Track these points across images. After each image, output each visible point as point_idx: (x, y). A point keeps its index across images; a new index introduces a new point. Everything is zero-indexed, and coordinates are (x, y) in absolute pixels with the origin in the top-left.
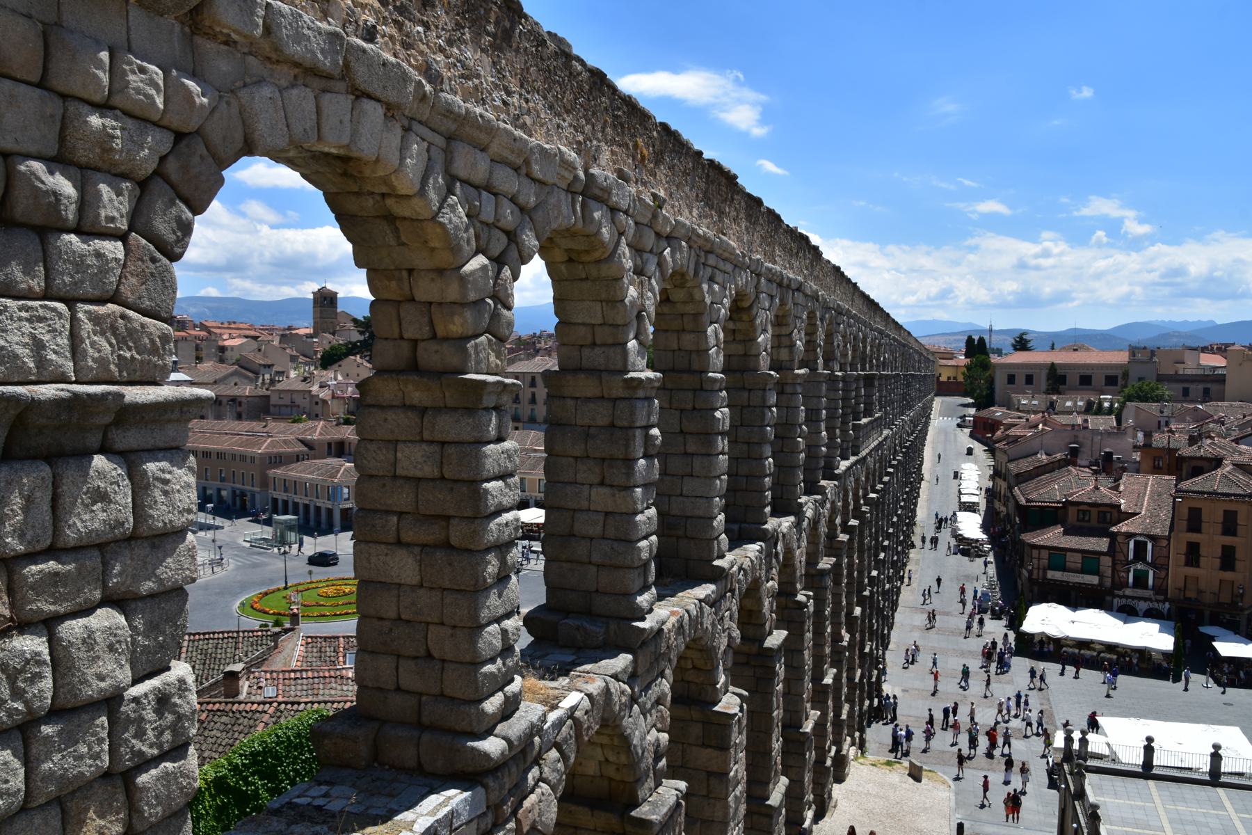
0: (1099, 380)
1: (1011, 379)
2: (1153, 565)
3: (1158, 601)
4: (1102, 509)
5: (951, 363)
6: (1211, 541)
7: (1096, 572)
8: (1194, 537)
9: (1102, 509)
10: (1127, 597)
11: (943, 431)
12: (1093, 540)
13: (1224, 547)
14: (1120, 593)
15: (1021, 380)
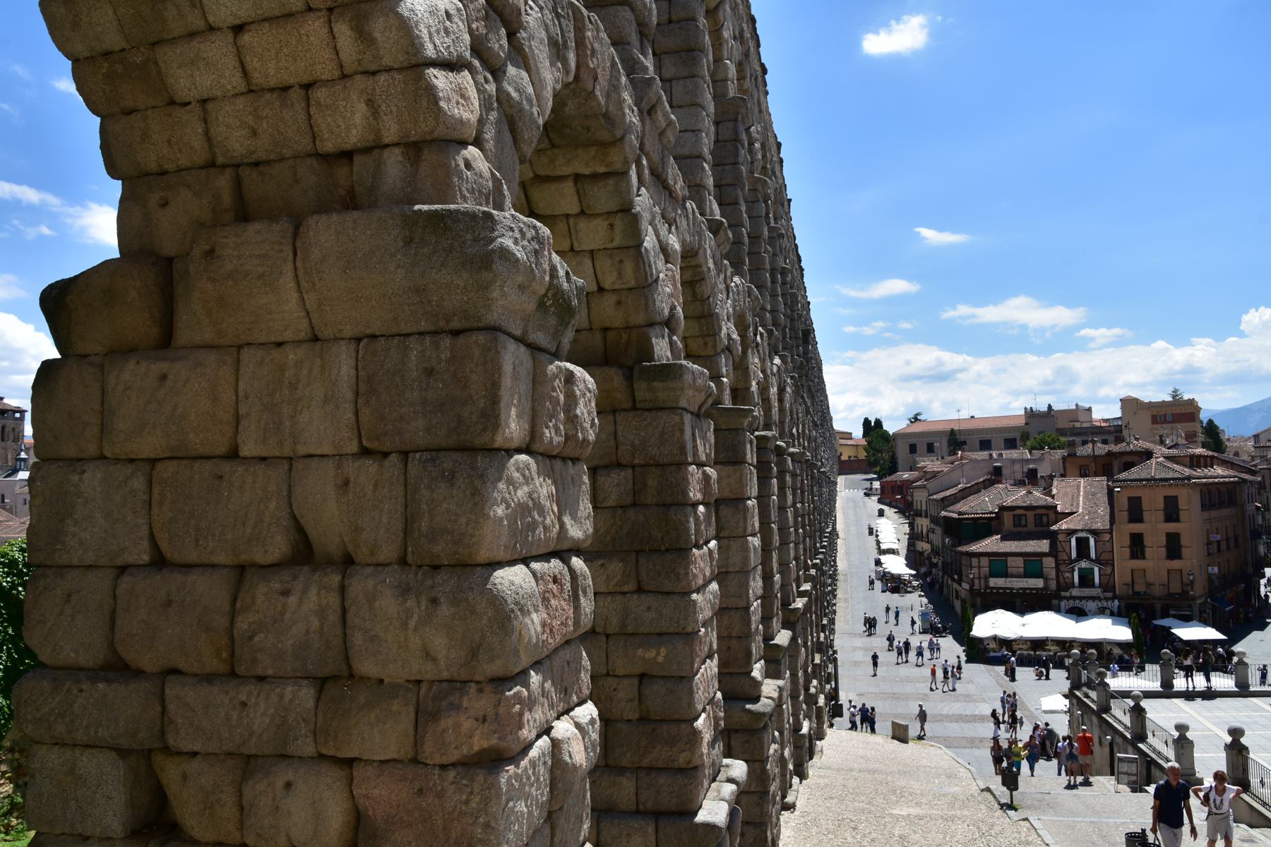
0: (998, 441)
1: (913, 448)
2: (1098, 561)
3: (1107, 599)
4: (1038, 511)
5: (850, 442)
6: (1155, 529)
7: (1039, 575)
8: (1137, 528)
9: (1038, 511)
10: (1074, 598)
11: (848, 500)
12: (1031, 542)
13: (1169, 535)
14: (1067, 594)
15: (922, 448)
